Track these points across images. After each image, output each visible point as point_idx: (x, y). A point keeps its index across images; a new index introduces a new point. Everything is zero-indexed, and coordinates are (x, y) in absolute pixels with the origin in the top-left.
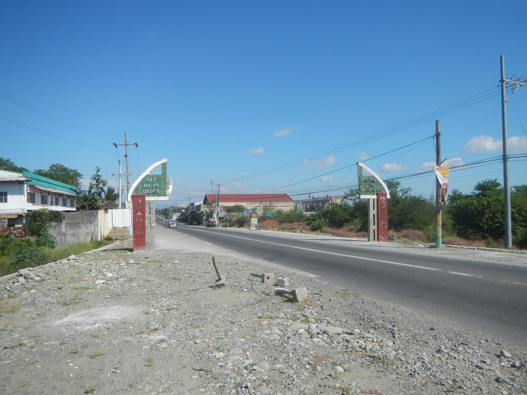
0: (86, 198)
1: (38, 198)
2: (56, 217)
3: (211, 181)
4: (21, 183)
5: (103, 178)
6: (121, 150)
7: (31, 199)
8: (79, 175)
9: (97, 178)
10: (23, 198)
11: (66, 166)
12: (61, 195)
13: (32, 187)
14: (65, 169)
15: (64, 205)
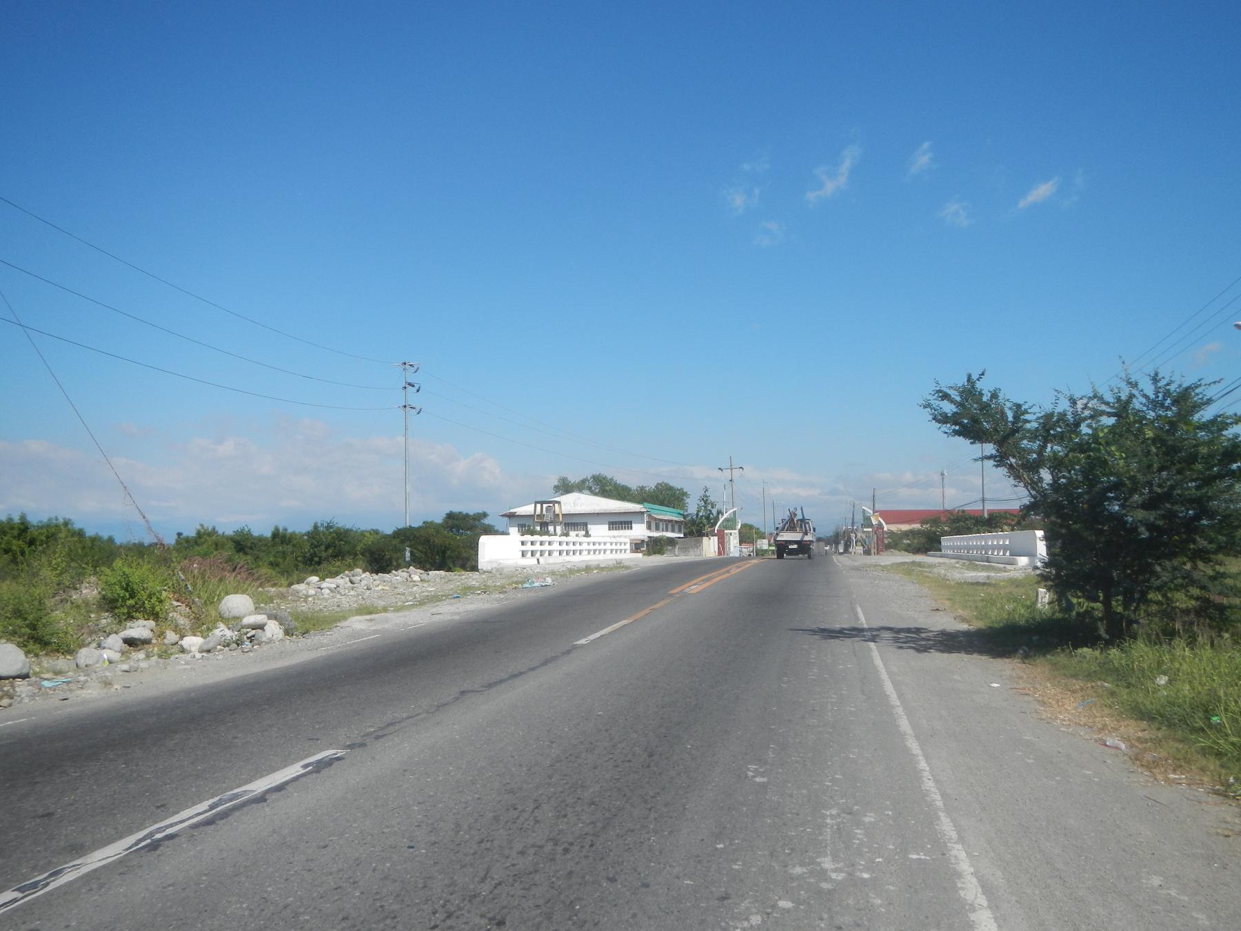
0: (693, 522)
1: (653, 526)
2: (671, 542)
3: (942, 474)
4: (642, 513)
5: (712, 499)
6: (727, 473)
7: (649, 528)
8: (685, 494)
9: (705, 500)
10: (644, 526)
11: (672, 483)
12: (671, 521)
13: (649, 516)
14: (671, 488)
15: (673, 531)
